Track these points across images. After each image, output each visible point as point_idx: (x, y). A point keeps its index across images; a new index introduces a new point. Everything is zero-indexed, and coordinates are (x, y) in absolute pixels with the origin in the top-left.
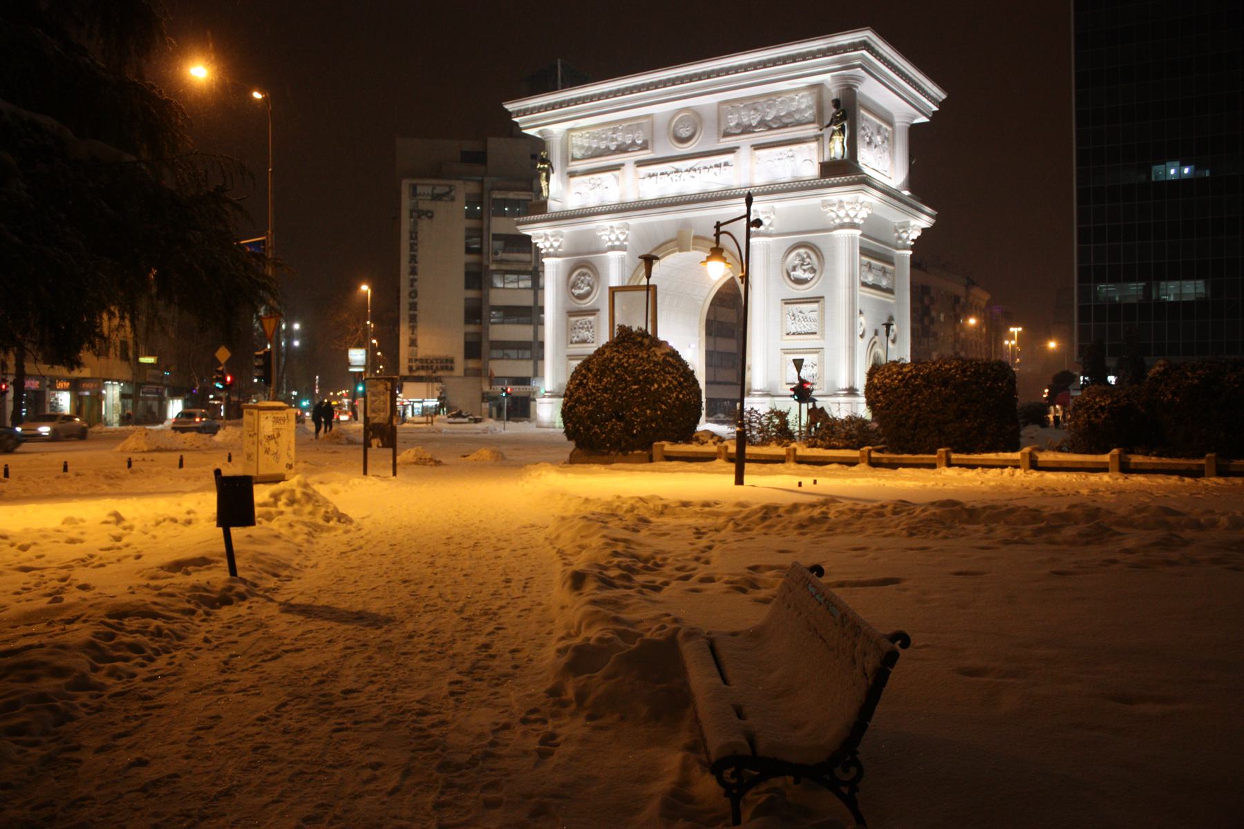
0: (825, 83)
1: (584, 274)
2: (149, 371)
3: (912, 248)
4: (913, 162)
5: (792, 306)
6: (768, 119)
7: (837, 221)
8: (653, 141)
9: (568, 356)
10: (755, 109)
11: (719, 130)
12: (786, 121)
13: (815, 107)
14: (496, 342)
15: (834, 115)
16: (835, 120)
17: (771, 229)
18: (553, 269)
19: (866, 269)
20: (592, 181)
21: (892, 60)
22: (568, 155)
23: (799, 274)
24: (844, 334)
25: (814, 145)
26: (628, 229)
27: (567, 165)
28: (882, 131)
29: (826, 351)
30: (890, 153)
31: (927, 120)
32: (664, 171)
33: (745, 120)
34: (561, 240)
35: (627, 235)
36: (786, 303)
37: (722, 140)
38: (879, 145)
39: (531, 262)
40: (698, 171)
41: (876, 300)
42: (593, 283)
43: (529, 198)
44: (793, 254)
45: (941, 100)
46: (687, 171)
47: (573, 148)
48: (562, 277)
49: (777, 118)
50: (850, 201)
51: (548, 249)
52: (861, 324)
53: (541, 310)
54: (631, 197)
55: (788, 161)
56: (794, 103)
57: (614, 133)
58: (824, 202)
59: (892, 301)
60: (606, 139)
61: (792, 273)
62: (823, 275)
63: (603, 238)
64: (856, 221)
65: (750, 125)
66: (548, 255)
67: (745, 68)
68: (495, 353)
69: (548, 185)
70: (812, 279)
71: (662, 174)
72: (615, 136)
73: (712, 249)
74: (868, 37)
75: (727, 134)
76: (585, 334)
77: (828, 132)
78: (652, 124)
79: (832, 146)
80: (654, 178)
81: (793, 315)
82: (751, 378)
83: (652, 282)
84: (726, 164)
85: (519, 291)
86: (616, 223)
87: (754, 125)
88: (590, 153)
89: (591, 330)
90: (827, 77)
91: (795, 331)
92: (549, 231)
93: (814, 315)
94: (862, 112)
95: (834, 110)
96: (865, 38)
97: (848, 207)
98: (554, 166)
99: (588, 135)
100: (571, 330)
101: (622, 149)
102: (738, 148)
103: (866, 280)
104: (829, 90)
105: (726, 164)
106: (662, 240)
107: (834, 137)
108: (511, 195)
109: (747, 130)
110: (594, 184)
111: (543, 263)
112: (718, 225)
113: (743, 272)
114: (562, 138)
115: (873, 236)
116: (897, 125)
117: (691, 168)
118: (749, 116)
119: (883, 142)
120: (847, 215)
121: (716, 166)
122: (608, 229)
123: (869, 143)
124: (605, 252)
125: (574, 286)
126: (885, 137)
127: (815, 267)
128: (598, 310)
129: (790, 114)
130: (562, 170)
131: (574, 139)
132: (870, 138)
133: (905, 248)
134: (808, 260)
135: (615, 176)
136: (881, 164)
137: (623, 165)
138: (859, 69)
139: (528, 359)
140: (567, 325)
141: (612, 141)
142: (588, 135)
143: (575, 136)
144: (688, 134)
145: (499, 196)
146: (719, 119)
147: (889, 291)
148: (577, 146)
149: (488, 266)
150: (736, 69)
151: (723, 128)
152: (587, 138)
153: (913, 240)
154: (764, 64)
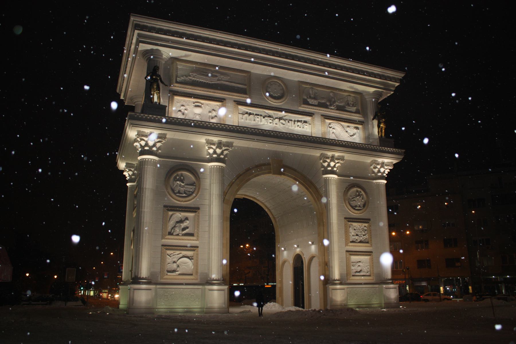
0: (364, 94)
29: (374, 254)
37: (303, 106)
40: (287, 121)
50: (388, 164)
58: (375, 161)
75: (306, 103)
84: (305, 122)
90: (372, 90)
102: (313, 114)
104: (365, 98)
105: (305, 122)
114: (165, 62)
121: (298, 121)
128: (198, 208)
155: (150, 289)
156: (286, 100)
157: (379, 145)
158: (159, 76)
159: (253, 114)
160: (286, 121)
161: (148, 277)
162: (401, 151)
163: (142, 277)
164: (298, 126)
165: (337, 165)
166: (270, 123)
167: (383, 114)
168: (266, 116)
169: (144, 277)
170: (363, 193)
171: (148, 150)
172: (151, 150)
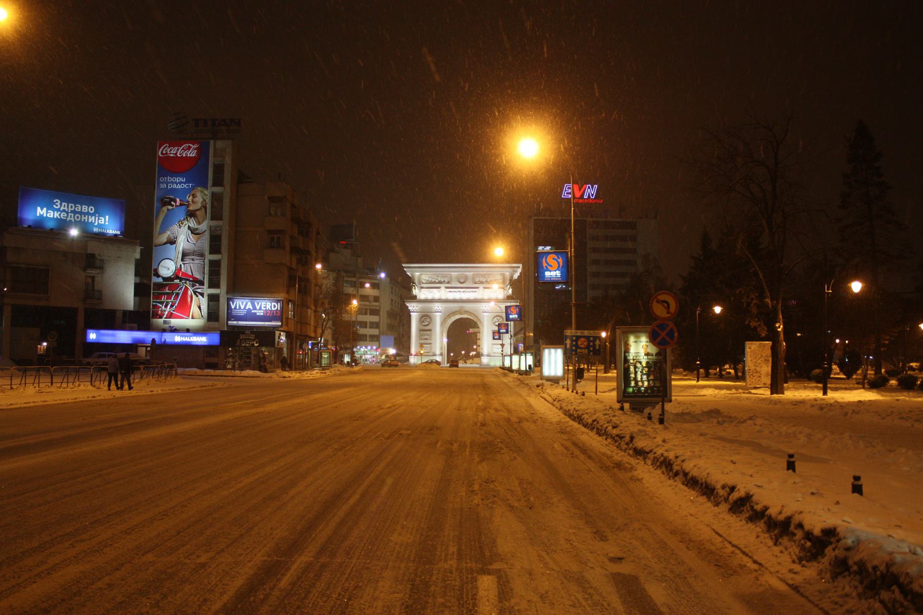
2: (307, 348)
18: (414, 317)
27: (420, 284)
33: (481, 280)
43: (355, 280)
44: (495, 319)
54: (444, 297)
60: (433, 278)
66: (414, 312)
75: (475, 283)
76: (426, 337)
78: (451, 278)
84: (475, 291)
101: (440, 282)
105: (475, 291)
106: (454, 311)
109: (482, 283)
121: (472, 292)
122: (437, 306)
125: (423, 322)
146: (473, 279)
158: (415, 283)
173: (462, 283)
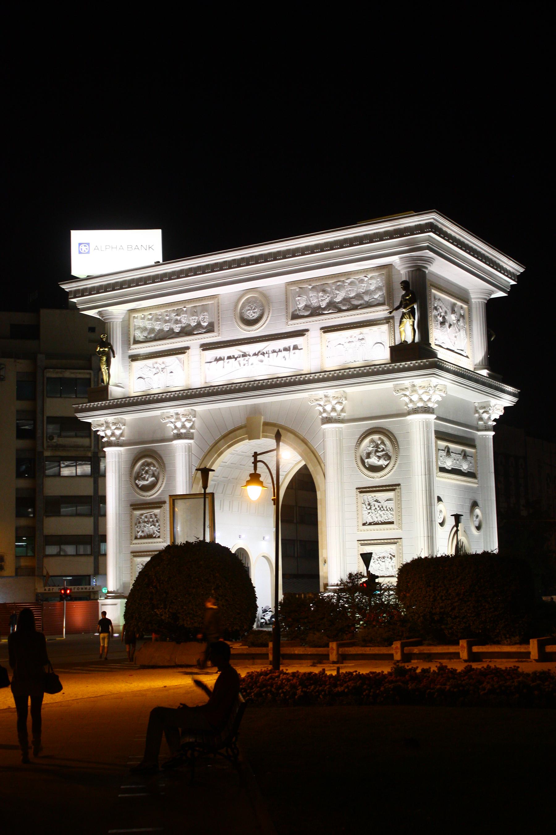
0: (393, 264)
1: (148, 464)
3: (495, 428)
4: (492, 339)
5: (368, 494)
6: (337, 301)
7: (411, 406)
8: (219, 323)
9: (132, 552)
10: (324, 291)
11: (287, 312)
12: (356, 302)
13: (384, 289)
14: (52, 536)
15: (403, 296)
16: (404, 303)
17: (343, 414)
19: (444, 454)
20: (156, 366)
21: (462, 239)
22: (129, 338)
23: (374, 461)
24: (422, 523)
25: (385, 328)
26: (195, 417)
27: (129, 348)
28: (456, 309)
30: (466, 330)
31: (506, 295)
32: (231, 355)
33: (314, 302)
34: (123, 427)
35: (194, 422)
36: (361, 492)
38: (454, 324)
39: (90, 447)
40: (266, 355)
41: (459, 486)
42: (159, 473)
43: (87, 376)
44: (367, 441)
45: (519, 274)
46: (255, 354)
47: (135, 330)
48: (125, 466)
49: (346, 300)
50: (423, 385)
51: (109, 437)
52: (441, 511)
53: (103, 499)
54: (197, 382)
55: (359, 343)
56: (363, 285)
57: (177, 315)
59: (476, 485)
61: (366, 461)
62: (398, 462)
63: (168, 425)
64: (430, 405)
65: (319, 307)
66: (110, 444)
67: (312, 249)
68: (51, 550)
69: (108, 369)
70: (387, 466)
71: (229, 358)
72: (179, 318)
73: (251, 475)
74: (433, 218)
75: (295, 317)
76: (150, 529)
77: (397, 315)
78: (218, 306)
79: (402, 329)
80: (221, 362)
81: (369, 504)
82: (327, 573)
83: (208, 491)
85: (78, 479)
86: (181, 410)
87: (322, 307)
88: (153, 335)
89: (157, 524)
91: (372, 521)
92: (111, 419)
93: (390, 504)
94: (433, 291)
95: (404, 292)
96: (432, 221)
97: (421, 391)
98: (115, 349)
99: (150, 317)
100: (136, 524)
101: (187, 332)
102: (307, 330)
103: (445, 466)
104: (399, 270)
105: (295, 348)
106: (230, 428)
107: (404, 320)
108: (68, 374)
109: (316, 312)
110: (158, 368)
111: (105, 452)
112: (256, 455)
113: (274, 496)
115: (451, 418)
116: (473, 301)
117: (259, 352)
118: (318, 298)
119: (458, 320)
120: (421, 399)
121: (286, 349)
123: (443, 323)
124: (172, 442)
125: (138, 476)
126: (461, 315)
127: (390, 454)
128: (164, 502)
129: (359, 296)
130: (123, 352)
131: (135, 320)
132: (444, 318)
133: (487, 429)
134: (383, 447)
135: (179, 360)
136: (456, 343)
137: (188, 348)
138: (427, 251)
139: (87, 555)
140: (131, 519)
141: (177, 324)
142: (150, 317)
143: (137, 318)
144: (256, 316)
145: (54, 375)
147: (471, 475)
148: (139, 328)
149: (43, 452)
150: (303, 251)
151: (291, 310)
152: (149, 320)
153: (495, 420)
154: (331, 246)
155: (115, 604)
156: (266, 323)
157: (390, 362)
159: (224, 359)
160: (264, 356)
161: (118, 590)
162: (427, 361)
163: (110, 591)
164: (284, 357)
165: (339, 408)
166: (244, 365)
167: (407, 298)
168: (240, 357)
169: (112, 591)
170: (387, 442)
171: (107, 441)
172: (109, 441)
173: (250, 323)
